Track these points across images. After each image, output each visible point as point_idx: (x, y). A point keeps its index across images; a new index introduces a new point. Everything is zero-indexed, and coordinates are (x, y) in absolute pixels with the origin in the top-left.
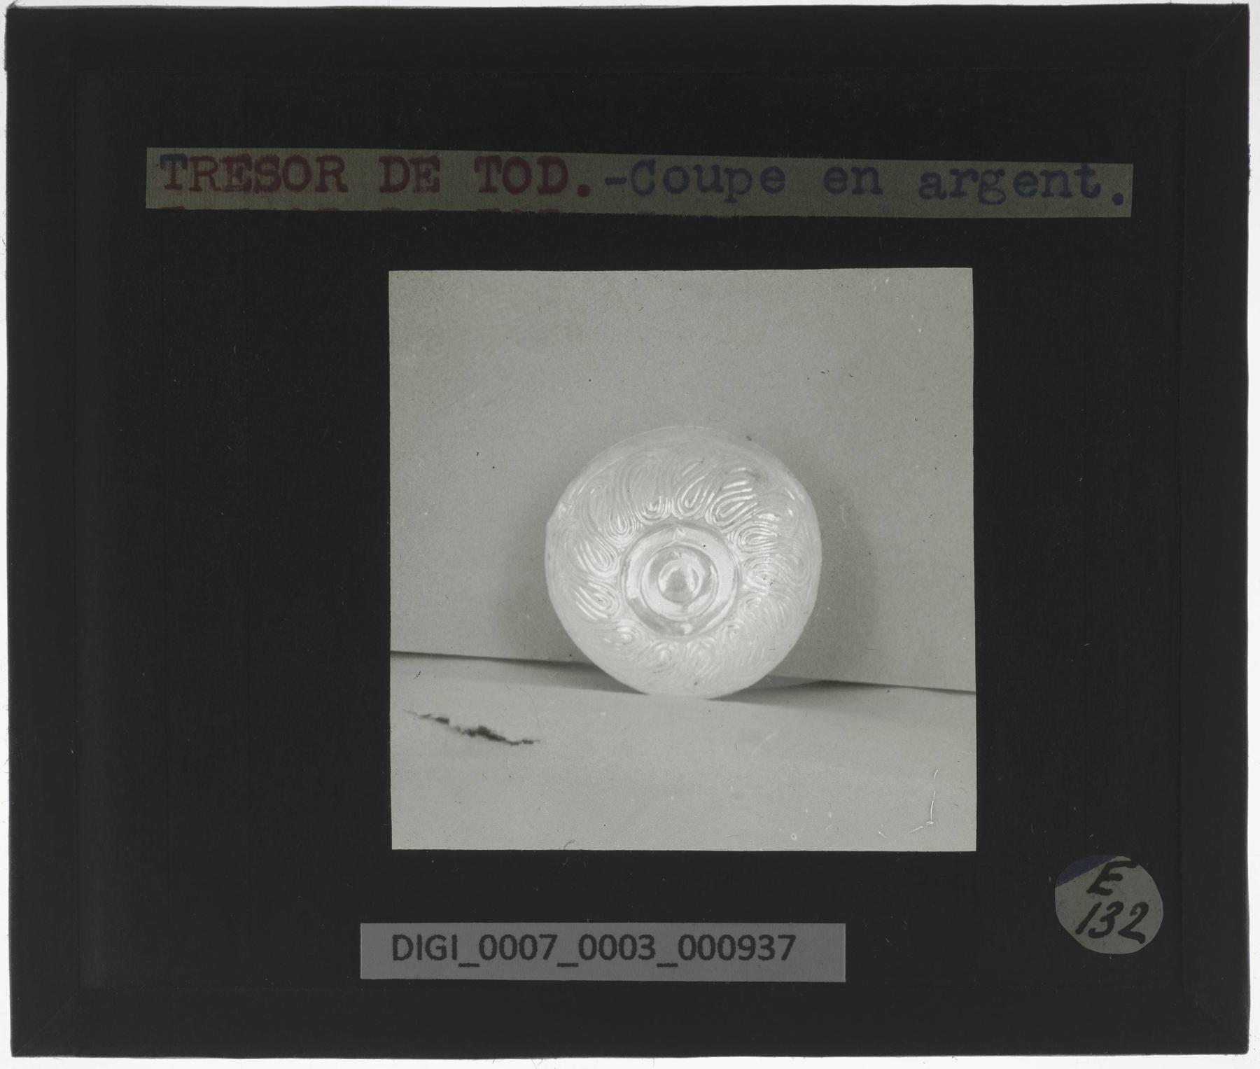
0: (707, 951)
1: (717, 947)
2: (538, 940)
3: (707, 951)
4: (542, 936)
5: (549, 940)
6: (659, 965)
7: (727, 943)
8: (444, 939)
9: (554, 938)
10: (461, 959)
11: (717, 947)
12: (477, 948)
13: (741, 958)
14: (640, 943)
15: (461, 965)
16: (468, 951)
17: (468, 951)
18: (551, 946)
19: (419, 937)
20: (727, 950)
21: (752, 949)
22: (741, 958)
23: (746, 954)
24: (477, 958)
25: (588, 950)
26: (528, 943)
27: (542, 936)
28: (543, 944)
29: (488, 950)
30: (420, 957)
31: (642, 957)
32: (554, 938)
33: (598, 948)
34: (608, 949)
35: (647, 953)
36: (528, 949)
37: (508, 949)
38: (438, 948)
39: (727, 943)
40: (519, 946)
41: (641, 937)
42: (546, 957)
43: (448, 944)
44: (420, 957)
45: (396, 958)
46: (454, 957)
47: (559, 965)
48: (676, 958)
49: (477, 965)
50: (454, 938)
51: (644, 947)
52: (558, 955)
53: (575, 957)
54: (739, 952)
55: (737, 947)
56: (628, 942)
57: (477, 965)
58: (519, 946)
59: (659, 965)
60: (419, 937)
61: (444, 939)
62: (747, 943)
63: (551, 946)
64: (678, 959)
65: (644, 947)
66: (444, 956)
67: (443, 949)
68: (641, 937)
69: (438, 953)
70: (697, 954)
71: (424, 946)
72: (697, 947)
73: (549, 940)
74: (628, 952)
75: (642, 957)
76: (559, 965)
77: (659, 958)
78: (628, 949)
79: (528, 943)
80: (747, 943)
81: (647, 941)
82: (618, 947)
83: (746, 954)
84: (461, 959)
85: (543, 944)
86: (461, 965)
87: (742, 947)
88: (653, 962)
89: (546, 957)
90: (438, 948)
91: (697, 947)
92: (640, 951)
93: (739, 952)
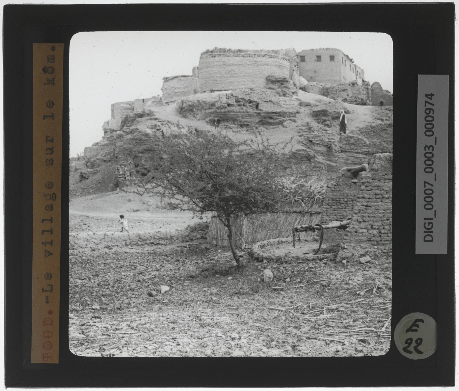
0: (431, 126)
1: (429, 122)
2: (426, 188)
3: (431, 126)
4: (425, 187)
5: (426, 184)
6: (436, 144)
7: (428, 119)
8: (425, 223)
9: (425, 182)
10: (432, 217)
11: (429, 122)
12: (427, 210)
13: (433, 113)
14: (427, 151)
15: (435, 217)
16: (430, 214)
17: (430, 214)
18: (428, 183)
19: (425, 232)
20: (430, 119)
21: (430, 109)
22: (433, 113)
23: (431, 111)
24: (433, 211)
25: (430, 170)
26: (427, 192)
27: (425, 187)
28: (428, 186)
29: (429, 207)
30: (432, 232)
31: (433, 150)
32: (425, 182)
33: (429, 166)
34: (430, 163)
35: (431, 148)
36: (430, 192)
37: (429, 199)
38: (429, 225)
39: (428, 119)
40: (429, 196)
41: (425, 150)
42: (432, 185)
43: (427, 221)
44: (432, 232)
45: (432, 241)
46: (432, 219)
47: (435, 181)
48: (433, 137)
49: (435, 211)
50: (425, 219)
51: (429, 150)
52: (432, 182)
53: (433, 174)
54: (431, 114)
55: (429, 115)
56: (428, 155)
57: (435, 211)
58: (429, 196)
59: (436, 144)
60: (425, 232)
61: (425, 223)
62: (428, 111)
63: (428, 183)
64: (433, 137)
65: (429, 150)
66: (432, 223)
67: (429, 223)
68: (425, 150)
69: (431, 225)
70: (432, 130)
71: (426, 230)
72: (430, 130)
73: (426, 184)
74: (431, 155)
75: (433, 150)
76: (435, 181)
77: (433, 144)
78: (431, 155)
79: (427, 192)
80: (428, 111)
81: (427, 148)
82: (429, 159)
83: (431, 111)
84: (432, 217)
85: (428, 186)
86: (435, 217)
87: (429, 113)
88: (435, 146)
89: (432, 185)
90: (429, 225)
91: (430, 130)
92: (431, 151)
93: (431, 114)
